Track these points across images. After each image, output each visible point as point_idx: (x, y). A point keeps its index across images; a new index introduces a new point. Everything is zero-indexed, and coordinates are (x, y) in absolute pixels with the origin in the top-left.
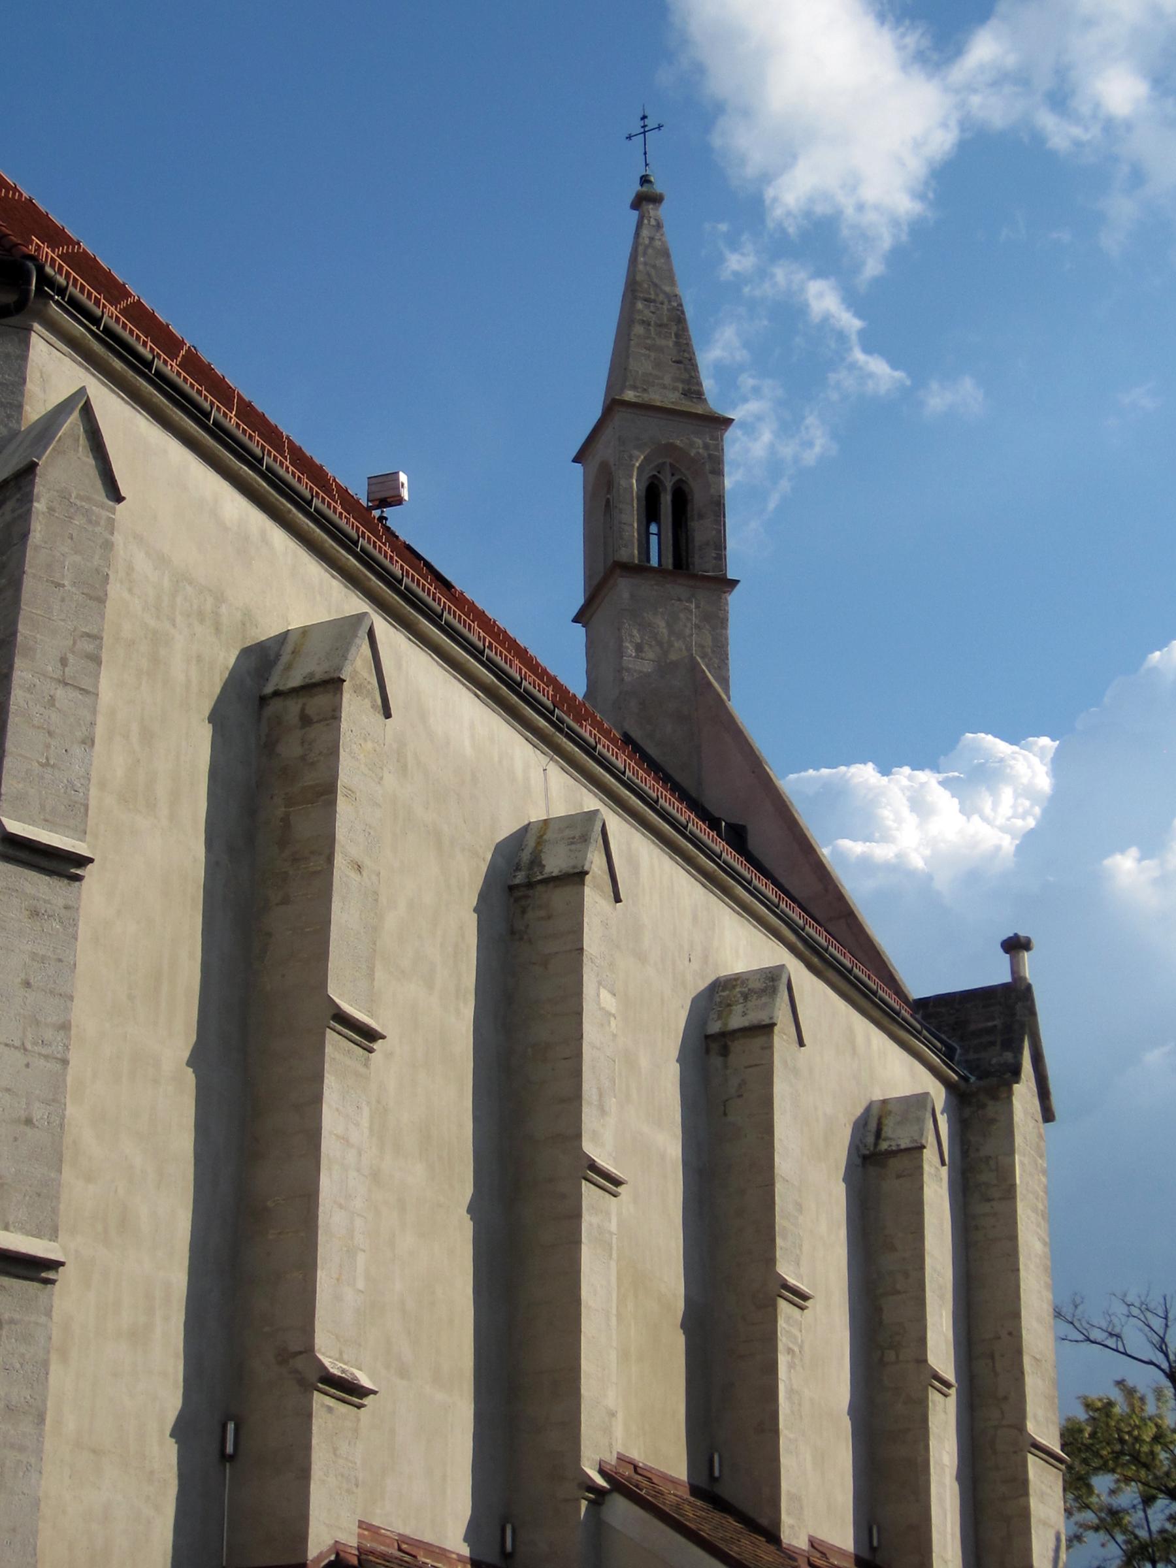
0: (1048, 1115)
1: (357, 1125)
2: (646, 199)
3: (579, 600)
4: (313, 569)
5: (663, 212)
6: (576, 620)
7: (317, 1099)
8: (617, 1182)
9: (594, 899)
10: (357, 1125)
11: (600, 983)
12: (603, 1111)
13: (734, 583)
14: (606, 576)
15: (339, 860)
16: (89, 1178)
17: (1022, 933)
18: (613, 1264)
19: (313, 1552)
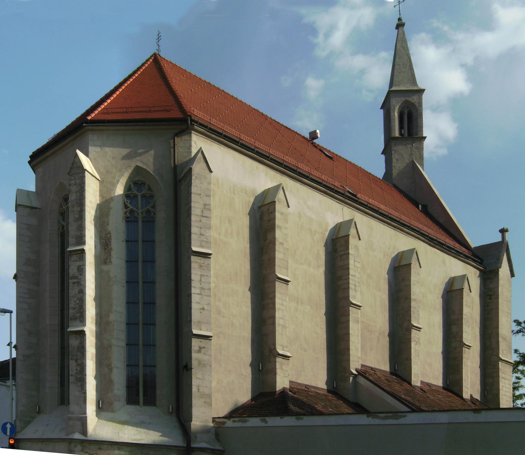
0: (512, 275)
1: (286, 301)
2: (400, 25)
3: (382, 147)
4: (272, 173)
5: (405, 28)
6: (382, 154)
7: (274, 297)
8: (360, 307)
9: (353, 241)
10: (286, 301)
11: (355, 261)
12: (356, 291)
13: (426, 137)
14: (389, 141)
15: (277, 243)
16: (224, 317)
17: (505, 227)
18: (359, 325)
19: (278, 389)
